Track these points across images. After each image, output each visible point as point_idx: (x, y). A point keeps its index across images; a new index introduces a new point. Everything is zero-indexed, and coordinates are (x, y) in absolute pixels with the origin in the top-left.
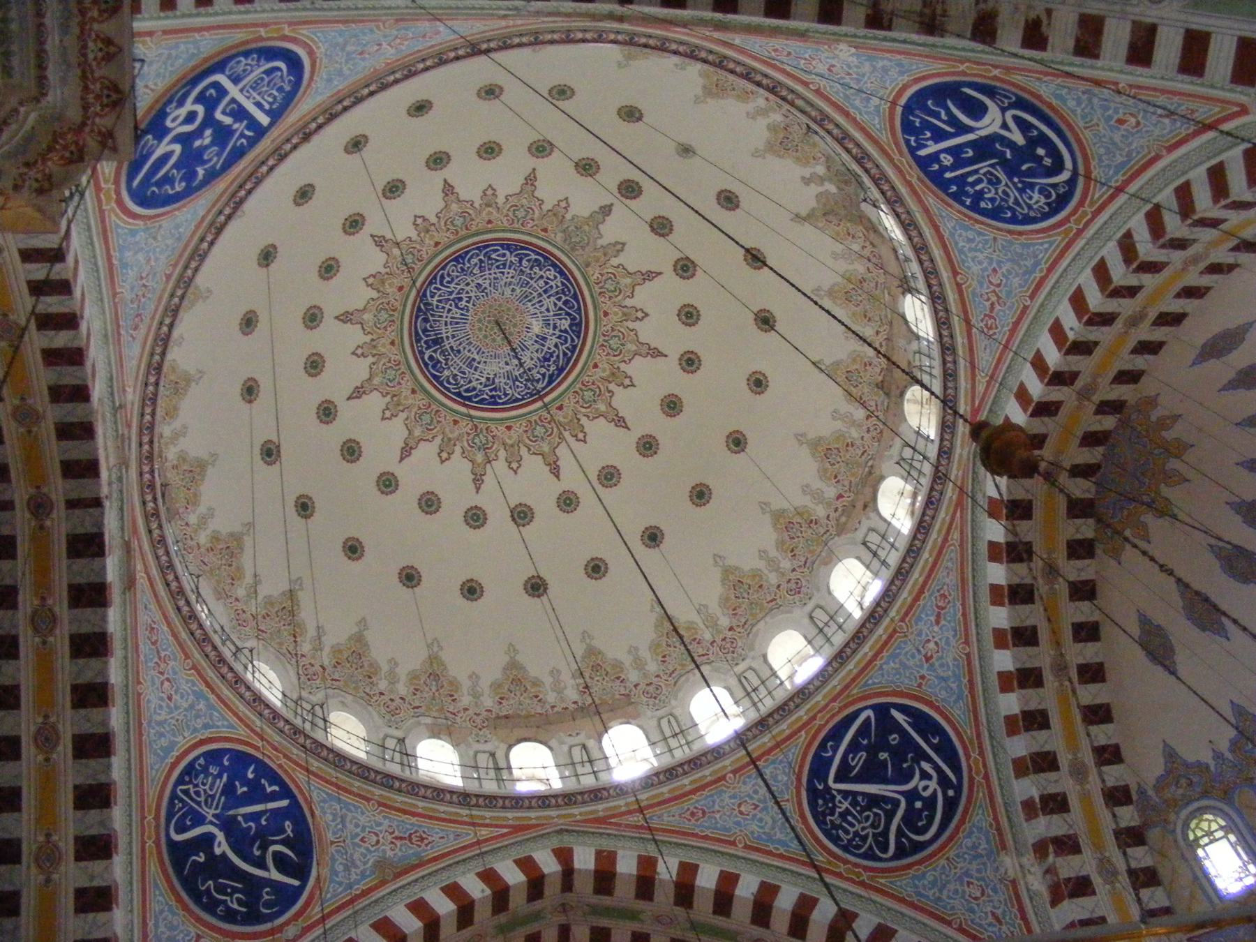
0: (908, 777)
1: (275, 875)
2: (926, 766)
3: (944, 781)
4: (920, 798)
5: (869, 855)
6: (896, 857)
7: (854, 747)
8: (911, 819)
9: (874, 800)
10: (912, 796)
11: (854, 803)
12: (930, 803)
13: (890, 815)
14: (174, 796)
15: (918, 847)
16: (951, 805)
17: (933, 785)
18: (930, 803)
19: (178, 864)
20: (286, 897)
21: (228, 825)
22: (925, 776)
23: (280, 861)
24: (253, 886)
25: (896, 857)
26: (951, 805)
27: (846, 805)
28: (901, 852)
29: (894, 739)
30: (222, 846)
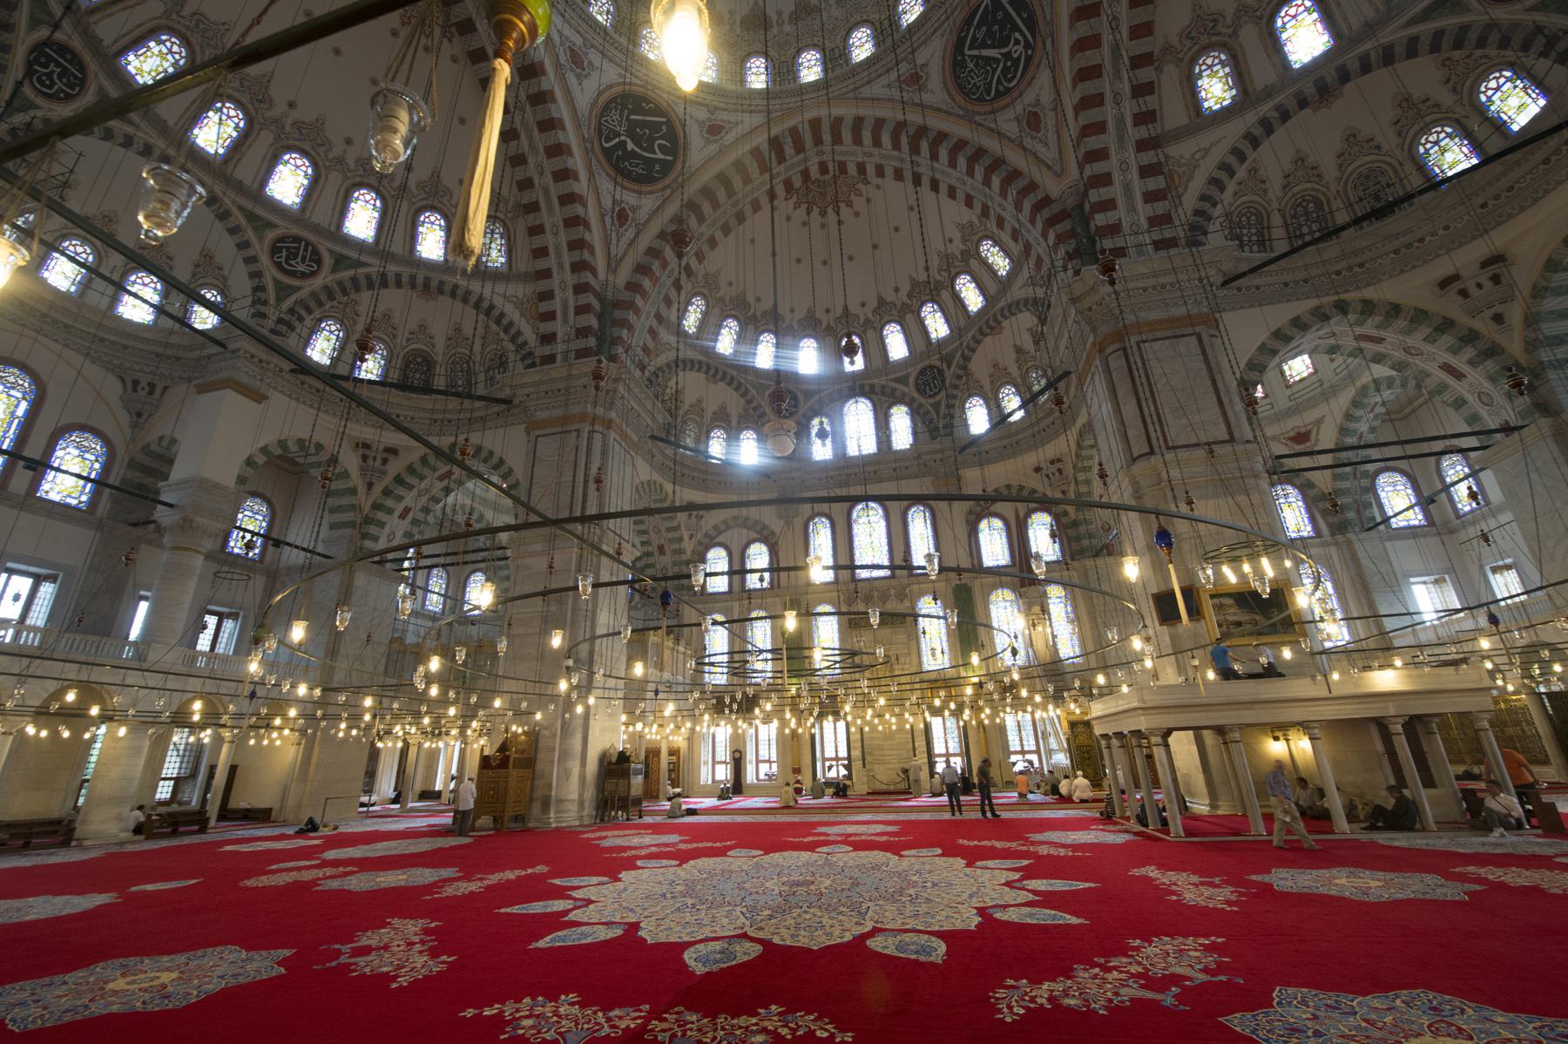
0: (1004, 42)
1: (660, 156)
2: (1017, 35)
3: (1027, 46)
4: (1011, 58)
5: (981, 100)
6: (996, 98)
7: (978, 27)
8: (1005, 71)
9: (988, 60)
10: (1007, 56)
11: (977, 65)
12: (1016, 62)
13: (994, 71)
14: (600, 124)
15: (1008, 90)
16: (1029, 59)
17: (1020, 48)
18: (1016, 62)
19: (609, 160)
20: (667, 167)
21: (631, 133)
22: (1017, 42)
23: (663, 149)
24: (649, 163)
25: (996, 98)
26: (1029, 59)
27: (971, 66)
28: (999, 95)
29: (1000, 15)
30: (630, 146)
